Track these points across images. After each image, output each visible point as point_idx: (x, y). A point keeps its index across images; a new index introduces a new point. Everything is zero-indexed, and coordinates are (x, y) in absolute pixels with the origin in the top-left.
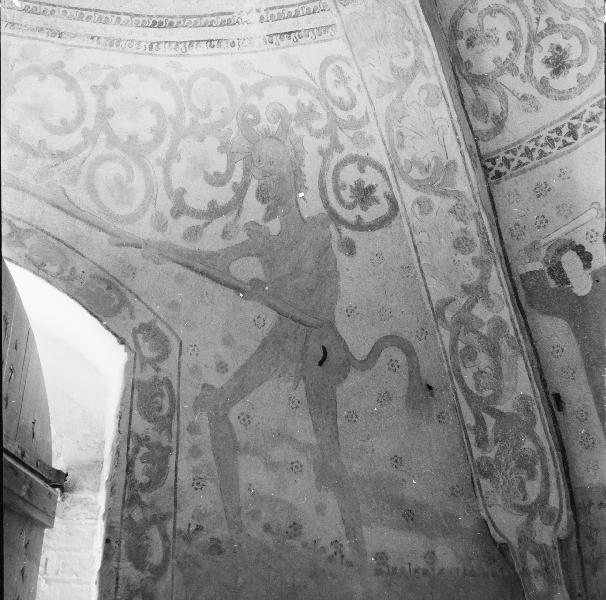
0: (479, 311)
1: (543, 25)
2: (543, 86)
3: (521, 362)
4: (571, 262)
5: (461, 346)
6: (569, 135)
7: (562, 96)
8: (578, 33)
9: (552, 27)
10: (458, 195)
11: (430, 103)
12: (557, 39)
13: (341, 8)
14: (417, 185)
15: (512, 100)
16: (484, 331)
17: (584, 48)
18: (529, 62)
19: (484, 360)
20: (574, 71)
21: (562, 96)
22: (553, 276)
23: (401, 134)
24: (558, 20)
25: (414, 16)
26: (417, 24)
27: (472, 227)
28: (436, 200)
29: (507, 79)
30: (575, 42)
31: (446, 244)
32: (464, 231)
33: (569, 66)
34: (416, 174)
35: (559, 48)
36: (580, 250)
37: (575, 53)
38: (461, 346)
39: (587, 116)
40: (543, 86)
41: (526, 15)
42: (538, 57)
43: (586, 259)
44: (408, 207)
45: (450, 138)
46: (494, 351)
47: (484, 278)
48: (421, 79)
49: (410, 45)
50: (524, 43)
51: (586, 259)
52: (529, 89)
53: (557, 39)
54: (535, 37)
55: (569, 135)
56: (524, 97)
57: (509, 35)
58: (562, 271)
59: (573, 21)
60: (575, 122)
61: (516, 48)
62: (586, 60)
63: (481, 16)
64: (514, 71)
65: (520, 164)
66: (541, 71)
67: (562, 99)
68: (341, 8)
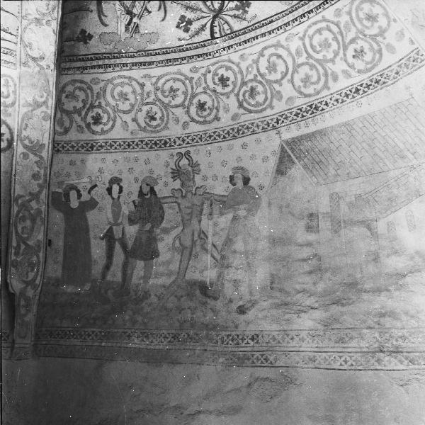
0: (34, 204)
1: (97, 103)
2: (88, 125)
3: (42, 228)
4: (73, 194)
5: (21, 215)
6: (90, 147)
7: (94, 133)
8: (109, 114)
9: (100, 106)
10: (41, 158)
11: (44, 119)
12: (100, 111)
13: (22, 67)
14: (25, 147)
15: (74, 125)
16: (32, 212)
17: (108, 121)
18: (86, 114)
19: (28, 223)
20: (101, 126)
21: (94, 133)
22: (65, 197)
23: (27, 125)
24: (103, 104)
25: (51, 83)
26: (51, 89)
27: (42, 172)
28: (31, 156)
29: (76, 116)
30: (106, 116)
31: (29, 174)
32: (38, 172)
33: (100, 123)
34: (27, 142)
35: (99, 115)
36: (78, 191)
37: (105, 120)
38: (21, 215)
39: (99, 144)
40: (88, 125)
41: (92, 96)
42: (90, 114)
43: (80, 196)
44: (19, 153)
45: (46, 135)
46: (33, 221)
47: (40, 192)
48: (44, 108)
49: (45, 95)
50: (88, 106)
51: (80, 196)
52: (83, 125)
53: (100, 111)
54: (92, 107)
55: (90, 147)
56: (79, 126)
57: (83, 101)
58: (69, 196)
59: (108, 108)
60: (94, 144)
61: (84, 107)
62: (106, 125)
63: (76, 88)
64: (80, 115)
65: (68, 150)
66: (89, 119)
67: (93, 134)
68: (22, 67)
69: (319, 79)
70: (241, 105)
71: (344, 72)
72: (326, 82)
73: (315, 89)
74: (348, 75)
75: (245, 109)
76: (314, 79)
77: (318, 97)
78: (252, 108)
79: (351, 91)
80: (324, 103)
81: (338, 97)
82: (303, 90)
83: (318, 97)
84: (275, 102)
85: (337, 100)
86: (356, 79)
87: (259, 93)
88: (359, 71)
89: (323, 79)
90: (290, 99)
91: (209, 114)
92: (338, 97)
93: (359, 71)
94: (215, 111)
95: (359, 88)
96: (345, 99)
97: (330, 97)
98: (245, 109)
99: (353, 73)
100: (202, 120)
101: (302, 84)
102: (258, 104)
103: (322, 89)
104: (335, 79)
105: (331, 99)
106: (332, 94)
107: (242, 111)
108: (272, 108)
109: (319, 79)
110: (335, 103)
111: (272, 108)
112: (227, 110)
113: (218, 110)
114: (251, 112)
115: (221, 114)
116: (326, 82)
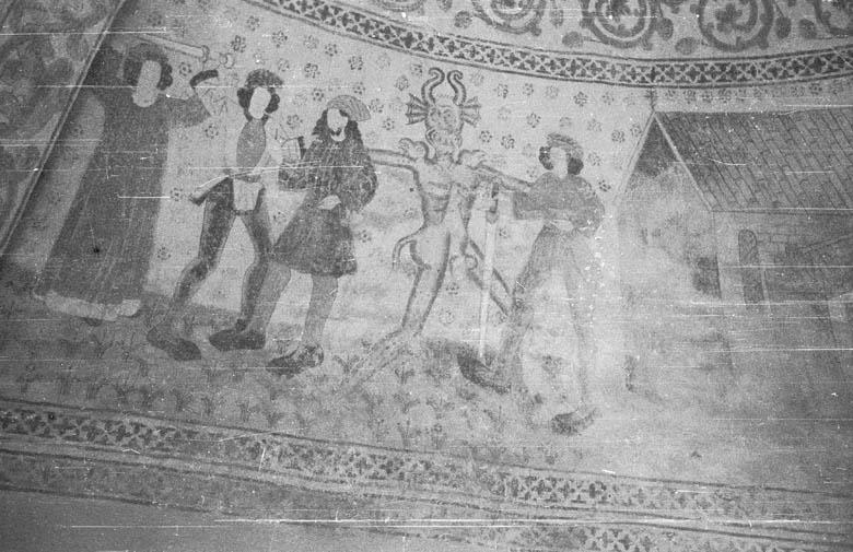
0: (58, 42)
3: (56, 117)
4: (150, 71)
5: (14, 55)
16: (48, 63)
19: (24, 88)
22: (126, 70)
36: (166, 71)
38: (14, 55)
43: (165, 81)
46: (40, 93)
47: (90, 21)
51: (165, 81)
58: (138, 71)
69: (752, 21)
70: (587, 22)
71: (805, 24)
72: (764, 33)
73: (738, 38)
74: (808, 30)
75: (596, 31)
76: (744, 19)
77: (740, 54)
78: (609, 35)
79: (806, 61)
80: (748, 68)
81: (779, 65)
82: (715, 33)
83: (740, 54)
84: (656, 38)
85: (774, 71)
86: (826, 43)
87: (628, 11)
88: (834, 31)
89: (759, 26)
90: (687, 43)
91: (521, 15)
92: (779, 65)
93: (834, 31)
94: (532, 13)
95: (824, 59)
96: (791, 72)
97: (762, 61)
98: (596, 31)
99: (820, 27)
100: (501, 21)
101: (716, 22)
102: (621, 31)
103: (750, 44)
104: (784, 32)
105: (763, 66)
106: (767, 57)
107: (586, 32)
108: (648, 47)
109: (752, 21)
110: (770, 75)
111: (648, 47)
112: (558, 22)
113: (539, 14)
114: (605, 41)
115: (545, 22)
116: (764, 33)
